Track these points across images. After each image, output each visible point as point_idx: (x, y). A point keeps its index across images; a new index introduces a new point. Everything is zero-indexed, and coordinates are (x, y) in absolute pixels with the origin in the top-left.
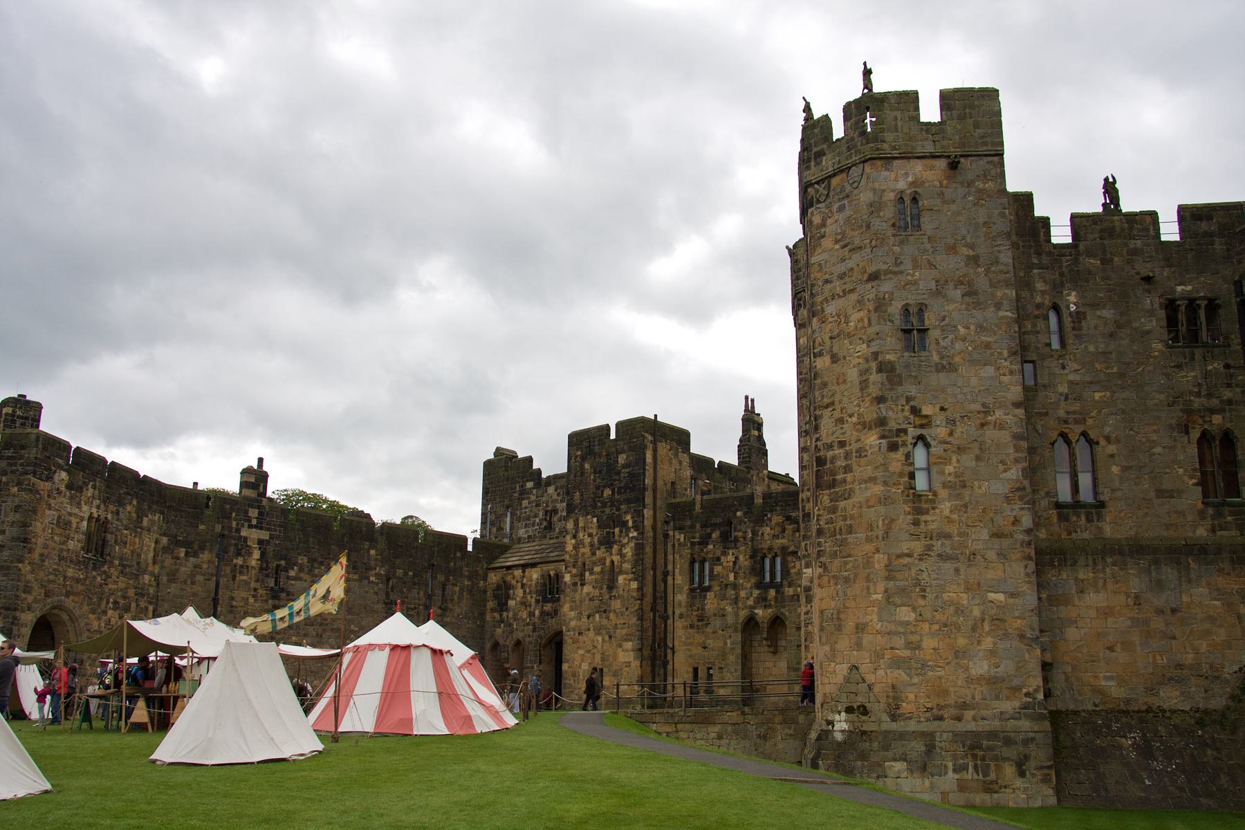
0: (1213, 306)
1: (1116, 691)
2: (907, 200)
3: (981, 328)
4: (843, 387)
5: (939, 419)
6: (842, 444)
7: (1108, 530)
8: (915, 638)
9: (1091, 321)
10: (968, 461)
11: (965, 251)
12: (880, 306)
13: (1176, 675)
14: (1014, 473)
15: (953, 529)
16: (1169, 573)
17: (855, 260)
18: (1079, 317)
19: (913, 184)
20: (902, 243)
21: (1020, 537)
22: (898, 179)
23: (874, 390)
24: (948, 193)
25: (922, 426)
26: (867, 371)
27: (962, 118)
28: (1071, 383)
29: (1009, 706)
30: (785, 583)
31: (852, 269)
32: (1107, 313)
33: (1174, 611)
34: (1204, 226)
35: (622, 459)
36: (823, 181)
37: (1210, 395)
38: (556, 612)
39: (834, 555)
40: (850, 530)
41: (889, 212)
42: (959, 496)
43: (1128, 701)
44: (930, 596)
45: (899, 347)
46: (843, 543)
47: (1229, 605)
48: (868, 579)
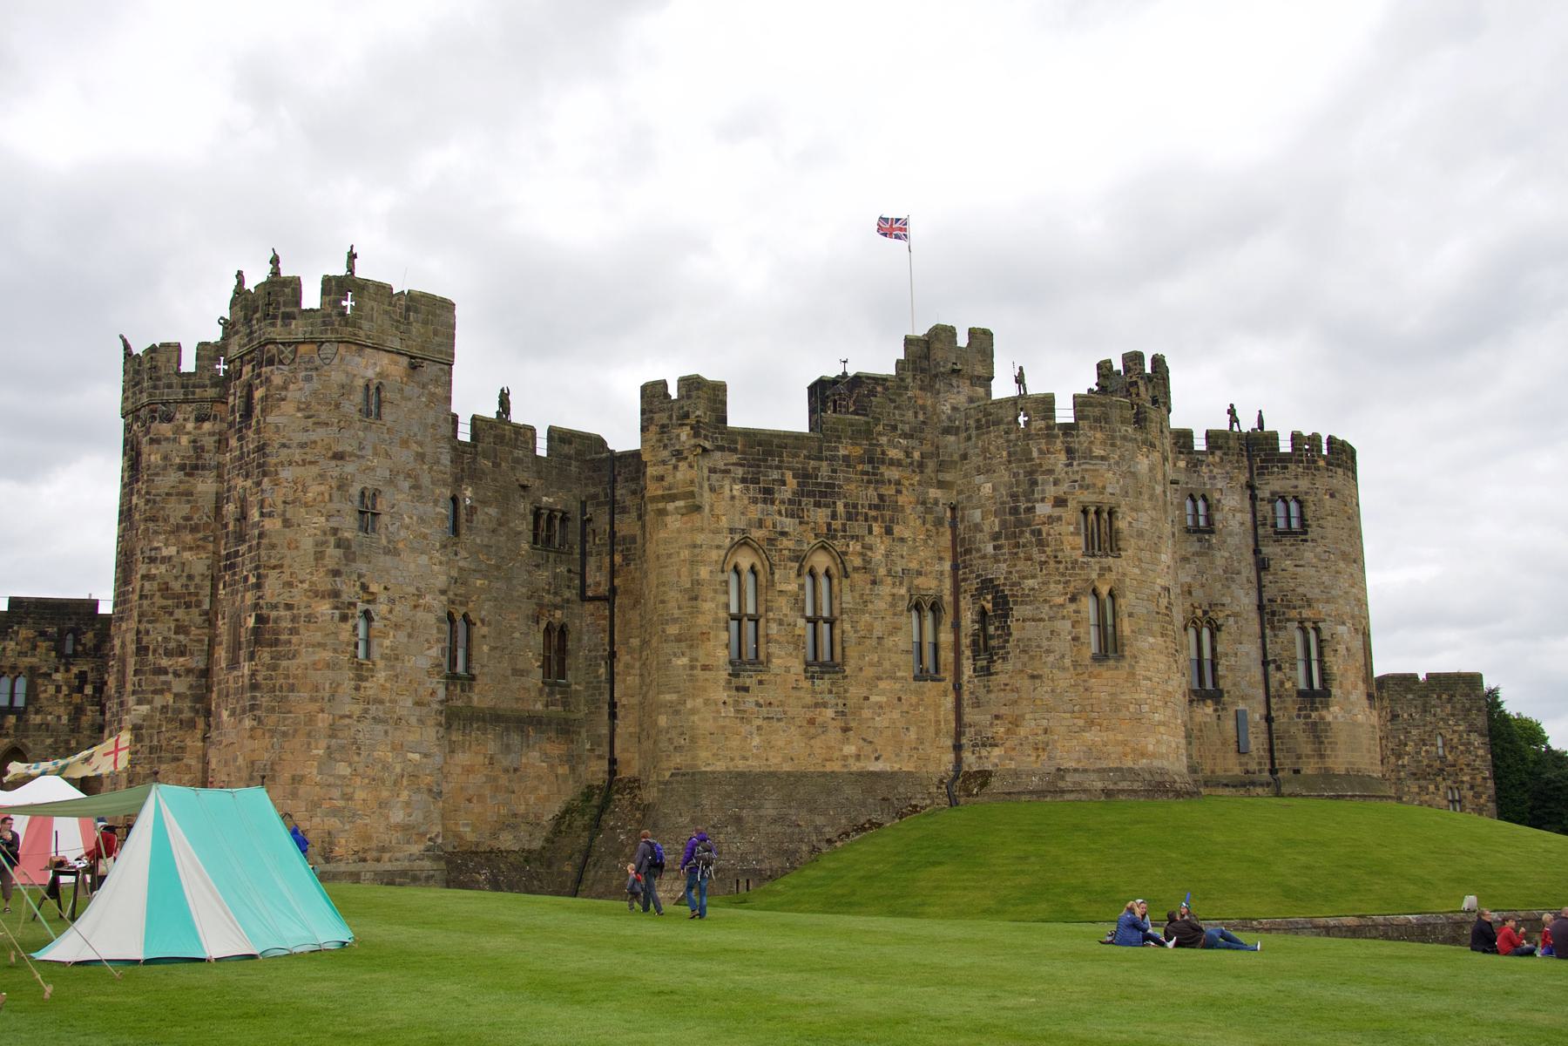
0: (564, 520)
1: (470, 835)
2: (373, 390)
3: (422, 520)
4: (295, 553)
5: (382, 597)
6: (289, 607)
7: (476, 700)
8: (350, 790)
9: (479, 517)
10: (402, 637)
11: (415, 447)
12: (342, 486)
13: (509, 823)
14: (435, 652)
15: (386, 696)
16: (515, 739)
17: (319, 434)
18: (472, 510)
19: (380, 375)
20: (366, 429)
21: (436, 706)
22: (369, 366)
23: (330, 563)
24: (406, 389)
25: (368, 602)
26: (325, 542)
27: (425, 323)
28: (461, 569)
29: (416, 849)
30: (31, 709)
31: (315, 442)
32: (492, 511)
33: (516, 770)
34: (566, 449)
36: (290, 344)
37: (556, 594)
39: (272, 710)
40: (292, 688)
41: (358, 397)
42: (393, 667)
43: (477, 845)
44: (364, 754)
45: (356, 526)
46: (283, 699)
47: (552, 766)
48: (309, 735)
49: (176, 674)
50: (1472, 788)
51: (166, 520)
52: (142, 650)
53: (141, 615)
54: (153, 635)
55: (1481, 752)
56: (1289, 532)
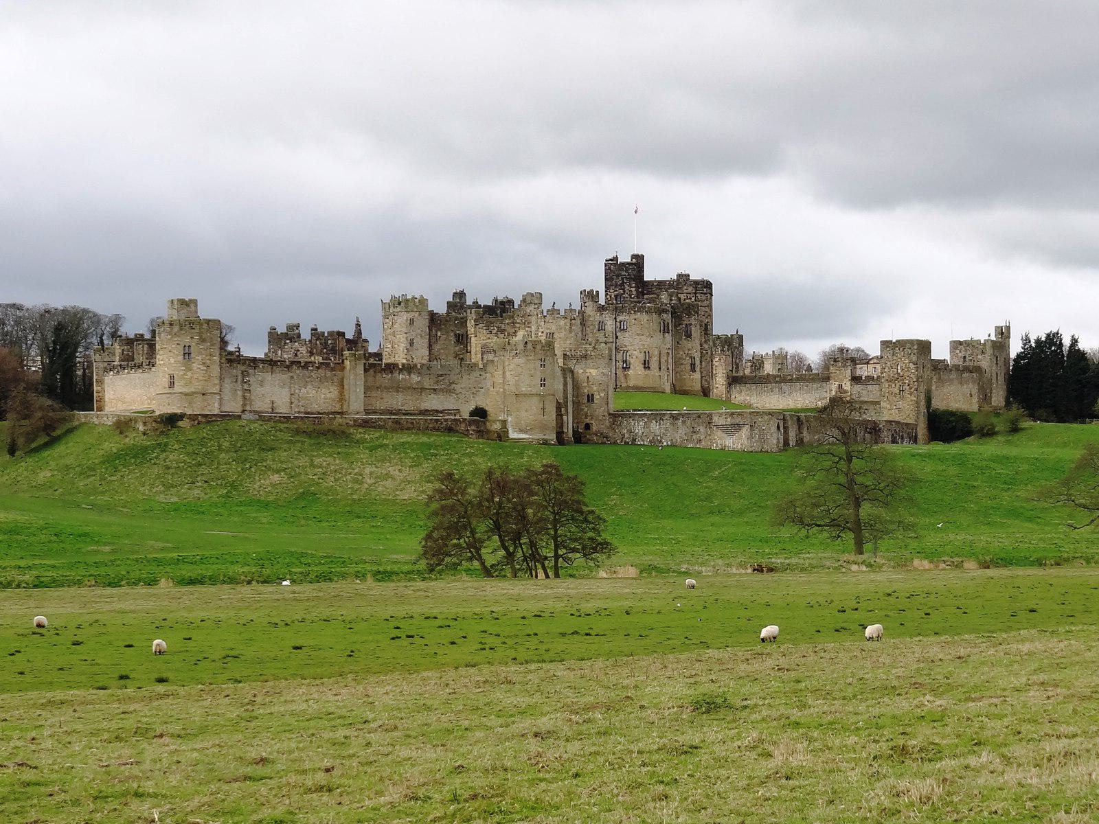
5: (415, 359)
35: (330, 342)
50: (909, 385)
55: (913, 371)
56: (623, 330)
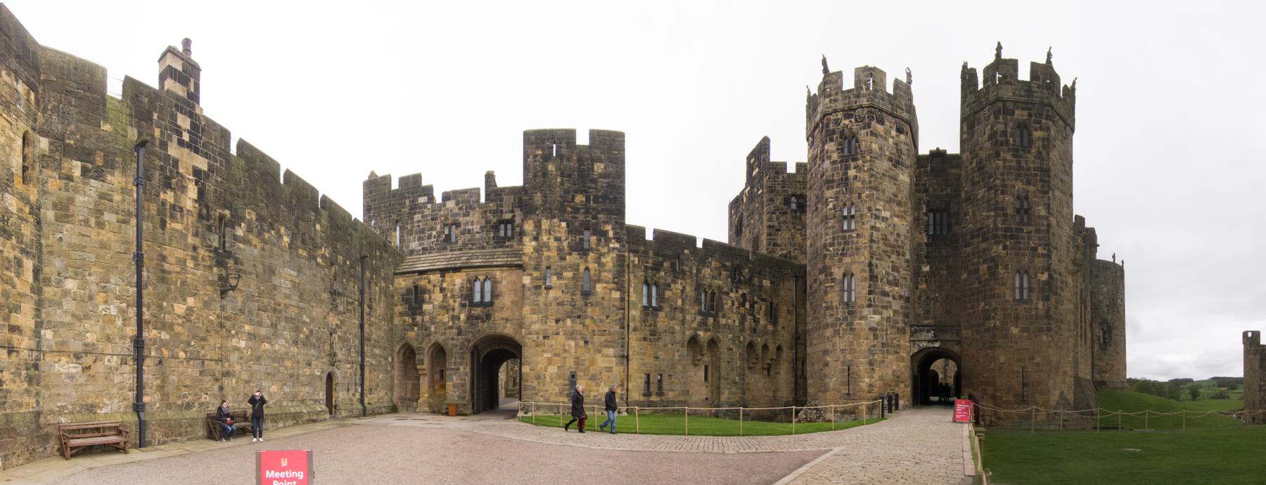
38: (488, 317)
49: (894, 297)
51: (883, 192)
52: (873, 277)
53: (872, 254)
54: (880, 268)
